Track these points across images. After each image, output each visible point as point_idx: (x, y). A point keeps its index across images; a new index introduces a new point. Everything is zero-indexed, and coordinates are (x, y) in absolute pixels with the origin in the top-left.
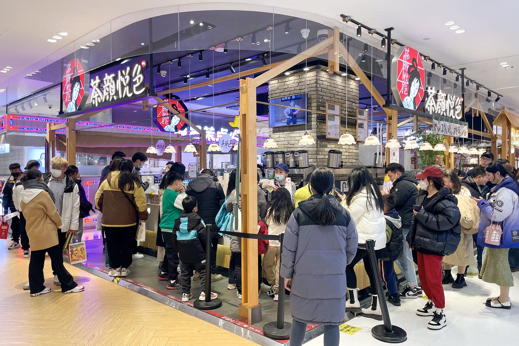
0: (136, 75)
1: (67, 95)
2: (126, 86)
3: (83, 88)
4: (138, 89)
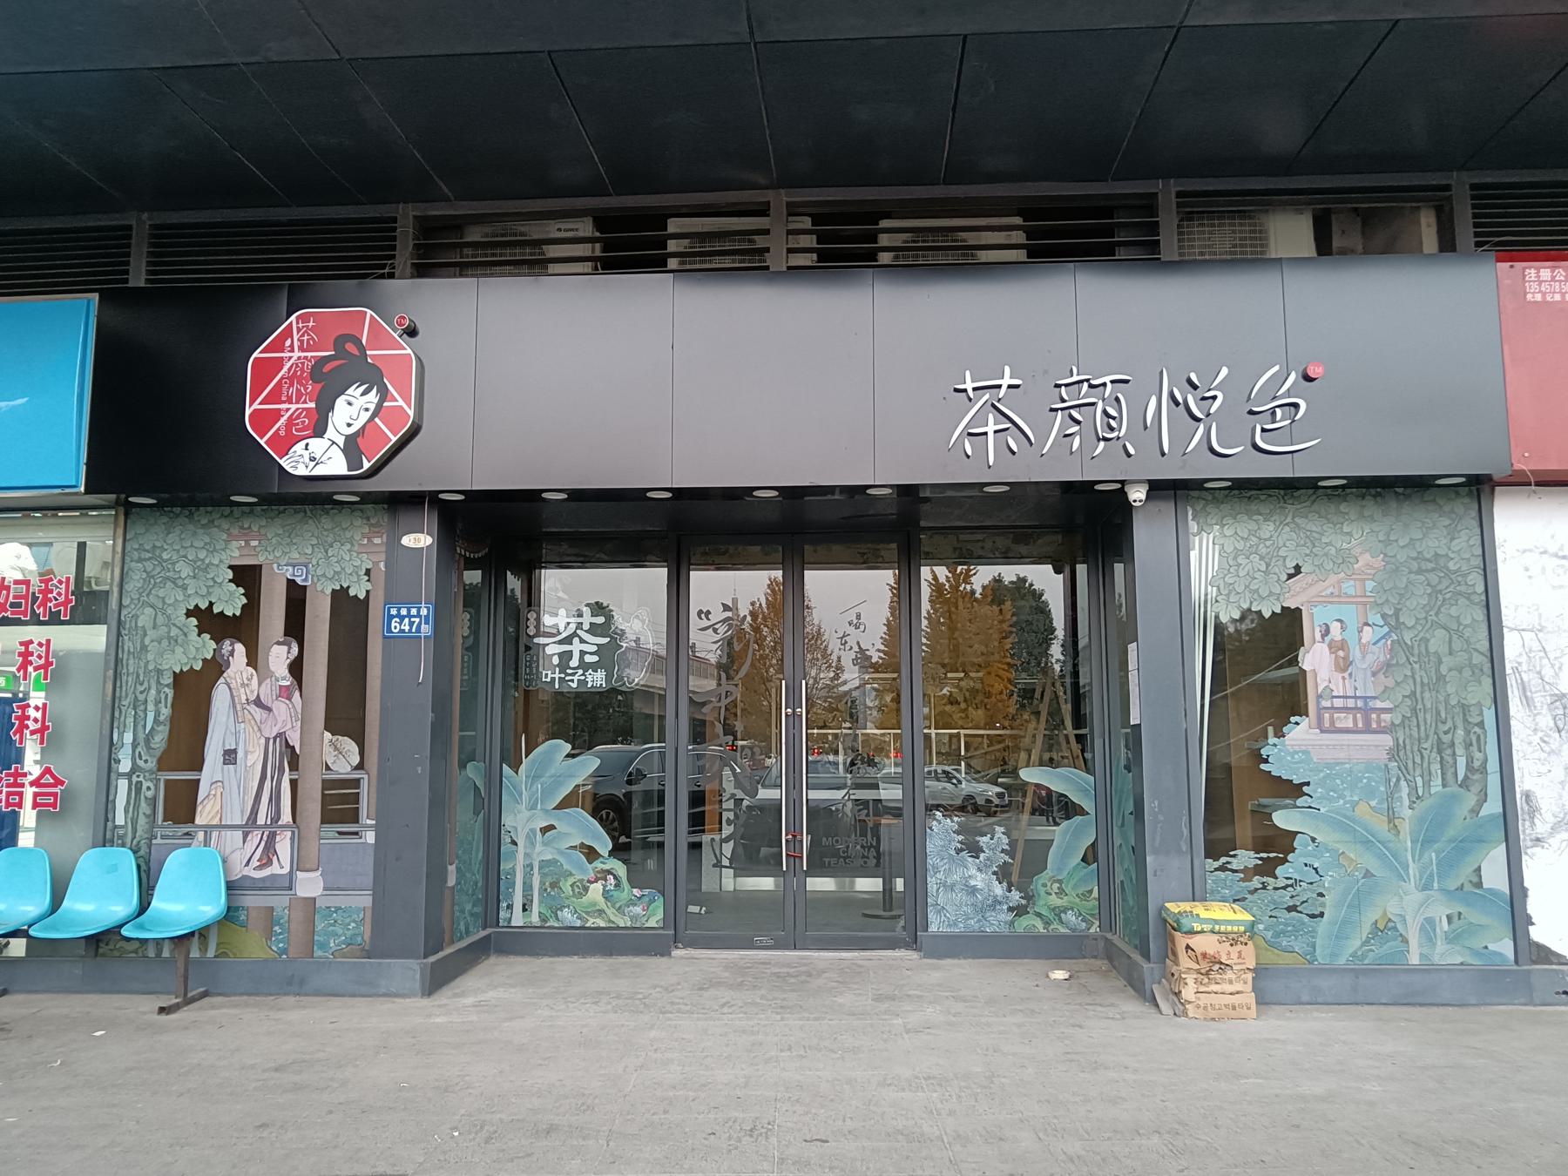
3: (401, 402)
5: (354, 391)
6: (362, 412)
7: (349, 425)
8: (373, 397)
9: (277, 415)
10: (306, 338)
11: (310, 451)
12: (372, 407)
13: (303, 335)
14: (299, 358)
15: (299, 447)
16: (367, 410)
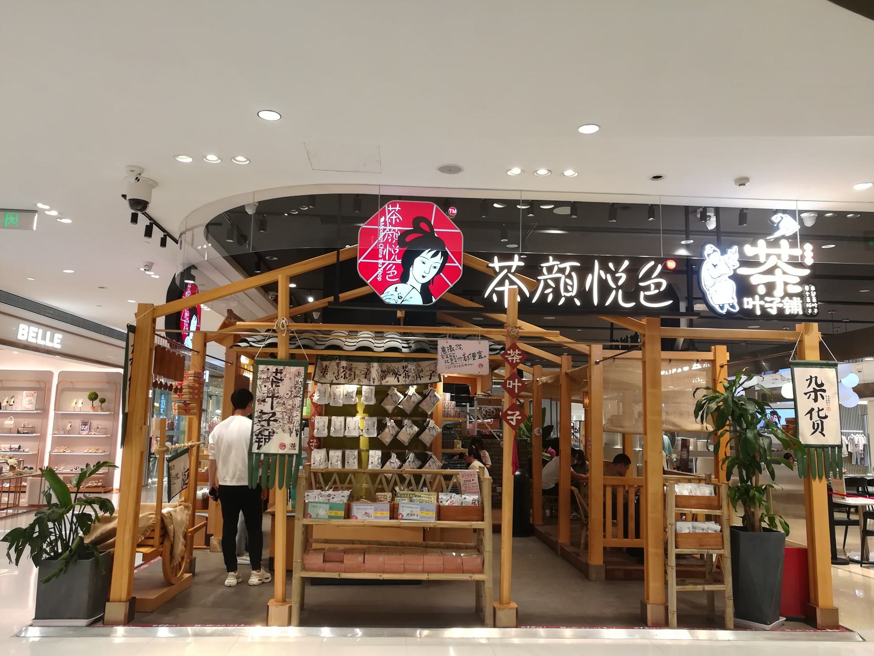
0: (648, 276)
1: (379, 266)
2: (617, 289)
3: (457, 264)
4: (648, 299)
5: (427, 254)
6: (432, 269)
7: (423, 277)
8: (439, 259)
9: (375, 267)
10: (394, 217)
11: (398, 292)
12: (438, 266)
13: (392, 215)
14: (390, 230)
15: (391, 289)
16: (435, 267)
